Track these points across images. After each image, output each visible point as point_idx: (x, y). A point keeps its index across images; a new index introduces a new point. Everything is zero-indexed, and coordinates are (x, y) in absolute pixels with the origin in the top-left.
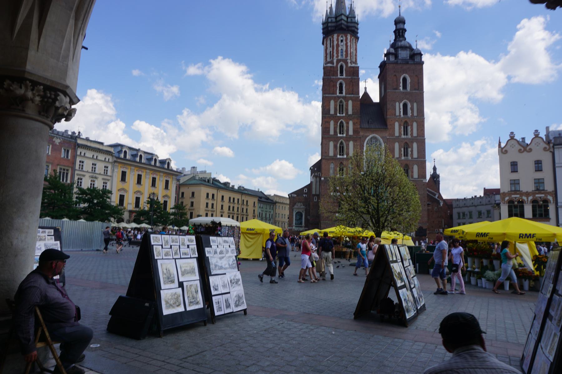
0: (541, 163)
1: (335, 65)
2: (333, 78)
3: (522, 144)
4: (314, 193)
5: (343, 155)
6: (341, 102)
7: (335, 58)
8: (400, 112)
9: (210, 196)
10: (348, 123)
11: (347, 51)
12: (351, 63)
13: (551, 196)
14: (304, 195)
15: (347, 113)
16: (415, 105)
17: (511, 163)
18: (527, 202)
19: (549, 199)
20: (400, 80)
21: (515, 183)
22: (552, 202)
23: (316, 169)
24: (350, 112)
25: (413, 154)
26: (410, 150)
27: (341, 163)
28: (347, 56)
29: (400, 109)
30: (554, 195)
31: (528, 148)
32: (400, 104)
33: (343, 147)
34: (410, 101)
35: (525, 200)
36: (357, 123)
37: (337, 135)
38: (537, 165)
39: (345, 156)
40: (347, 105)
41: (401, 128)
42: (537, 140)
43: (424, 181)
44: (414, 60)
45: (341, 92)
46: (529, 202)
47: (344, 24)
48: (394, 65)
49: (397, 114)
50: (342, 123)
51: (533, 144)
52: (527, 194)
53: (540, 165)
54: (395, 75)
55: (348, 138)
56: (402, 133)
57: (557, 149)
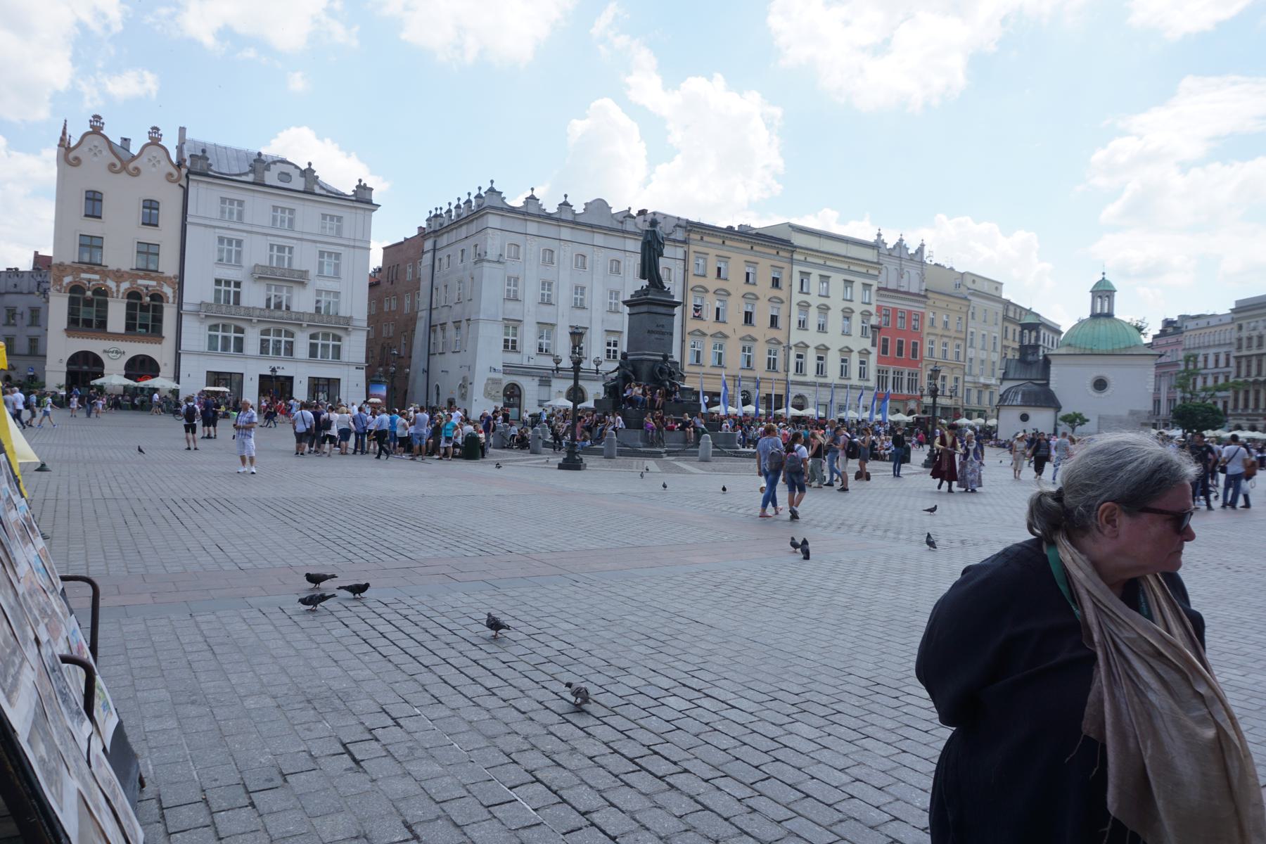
0: (158, 209)
3: (121, 152)
13: (169, 285)
17: (87, 192)
18: (115, 295)
19: (166, 294)
21: (91, 244)
22: (171, 300)
30: (177, 286)
31: (131, 166)
35: (111, 288)
38: (148, 211)
42: (154, 151)
46: (120, 295)
51: (144, 159)
52: (119, 276)
53: (155, 212)
57: (195, 184)
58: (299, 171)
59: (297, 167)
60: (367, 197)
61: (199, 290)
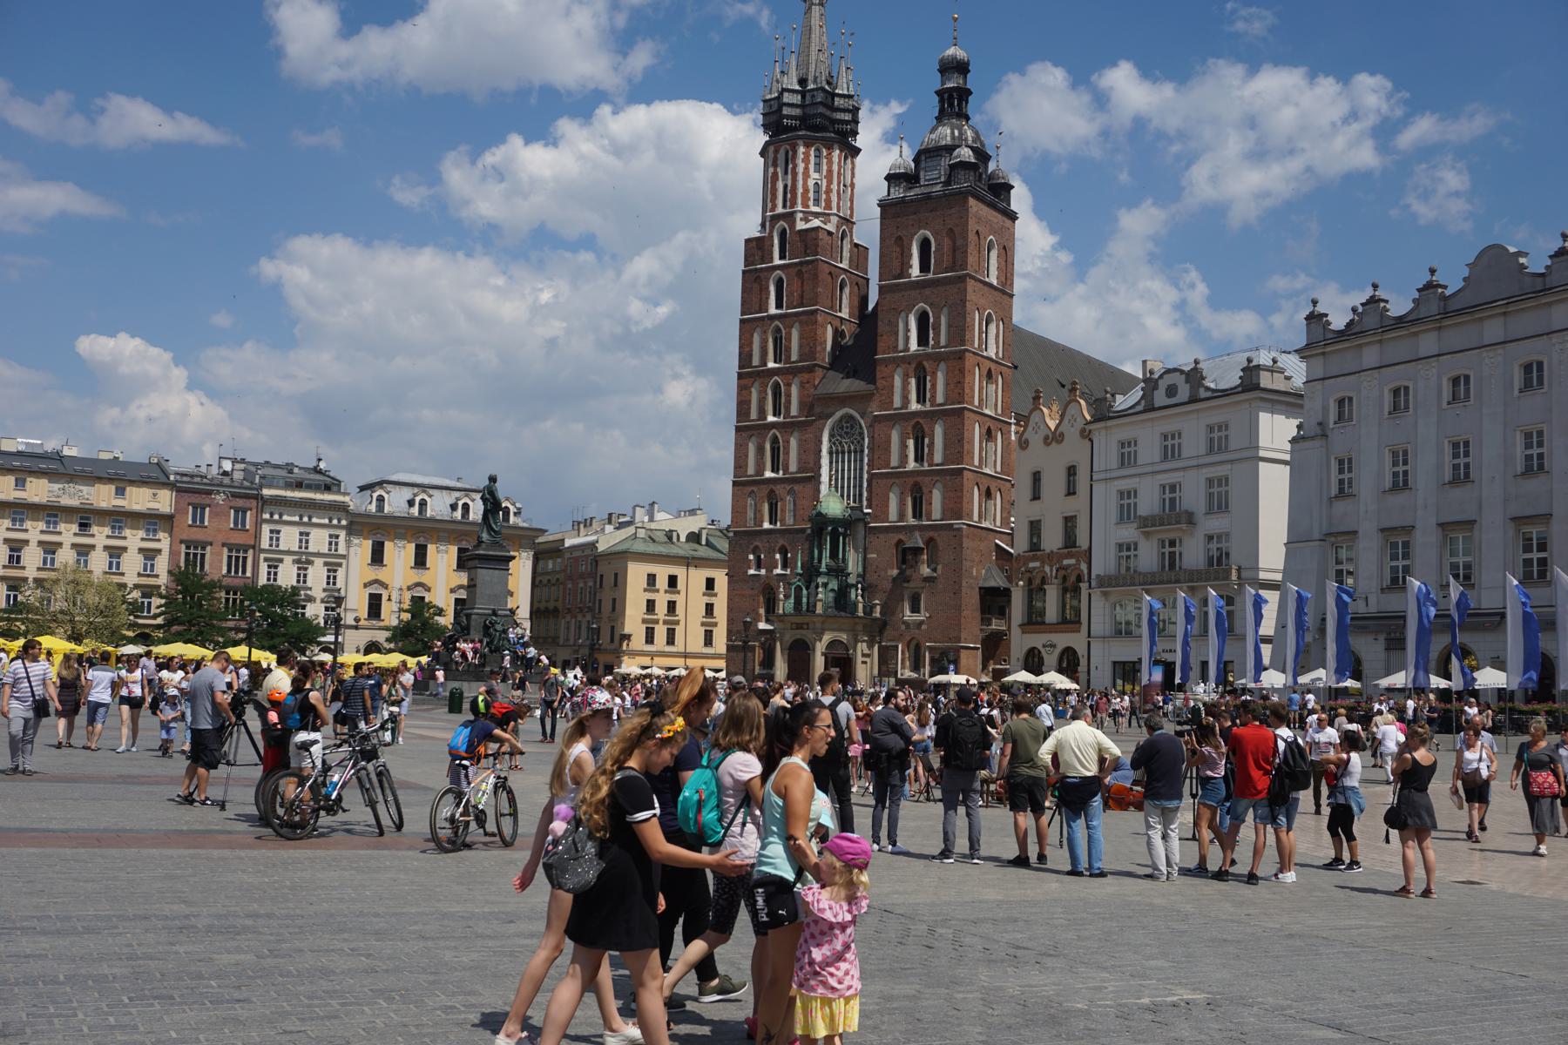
1: (767, 231)
2: (762, 269)
5: (777, 472)
6: (778, 330)
8: (907, 339)
9: (662, 583)
10: (788, 385)
12: (806, 220)
15: (788, 360)
20: (910, 249)
24: (794, 357)
26: (926, 440)
27: (772, 491)
28: (794, 204)
29: (907, 330)
32: (907, 317)
33: (779, 448)
34: (931, 305)
36: (808, 382)
37: (765, 418)
39: (781, 472)
40: (789, 334)
41: (909, 383)
43: (955, 526)
47: (788, 117)
49: (901, 347)
50: (777, 386)
52: (1051, 557)
55: (789, 427)
56: (913, 396)
58: (1184, 376)
59: (1182, 372)
60: (1254, 382)
61: (1103, 562)
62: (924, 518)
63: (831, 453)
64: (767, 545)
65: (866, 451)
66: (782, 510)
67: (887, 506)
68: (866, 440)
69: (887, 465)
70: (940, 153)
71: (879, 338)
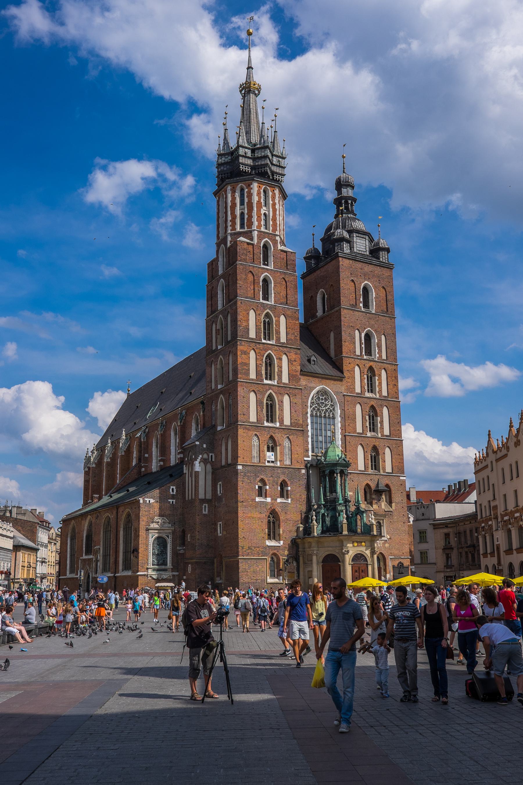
4: (201, 496)
7: (254, 227)
10: (280, 359)
11: (274, 219)
14: (169, 500)
15: (278, 339)
16: (383, 337)
23: (205, 446)
24: (283, 339)
25: (383, 428)
26: (379, 419)
27: (272, 438)
34: (376, 331)
44: (379, 259)
45: (266, 297)
48: (351, 262)
54: (353, 281)
62: (381, 471)
63: (312, 415)
64: (271, 478)
65: (339, 419)
66: (281, 453)
67: (357, 459)
68: (338, 412)
69: (355, 431)
70: (364, 236)
71: (343, 343)
